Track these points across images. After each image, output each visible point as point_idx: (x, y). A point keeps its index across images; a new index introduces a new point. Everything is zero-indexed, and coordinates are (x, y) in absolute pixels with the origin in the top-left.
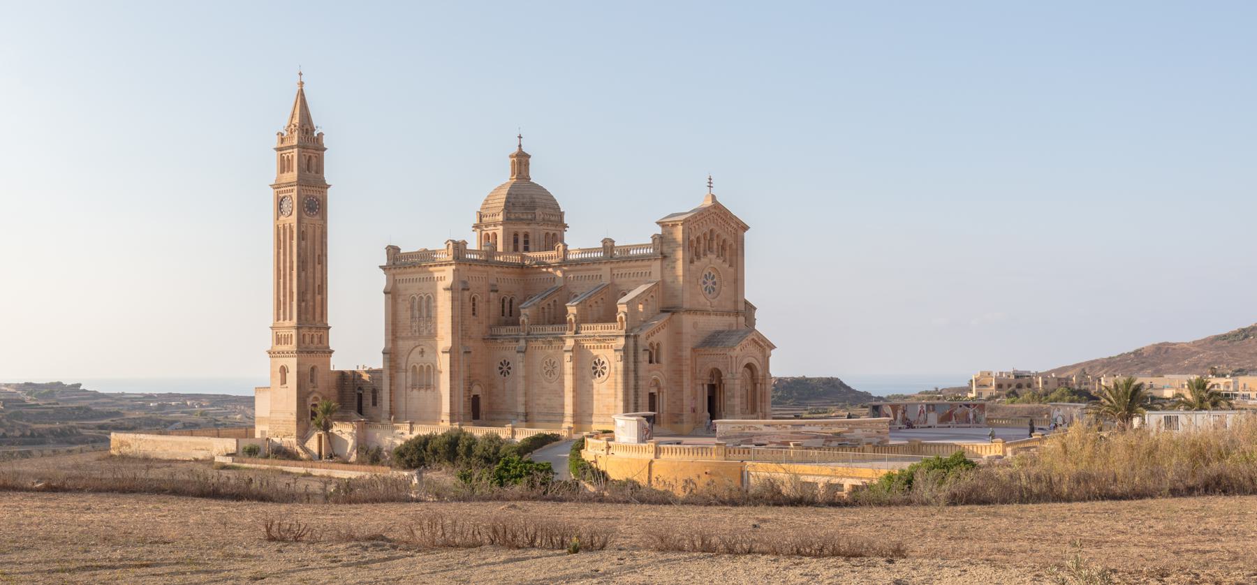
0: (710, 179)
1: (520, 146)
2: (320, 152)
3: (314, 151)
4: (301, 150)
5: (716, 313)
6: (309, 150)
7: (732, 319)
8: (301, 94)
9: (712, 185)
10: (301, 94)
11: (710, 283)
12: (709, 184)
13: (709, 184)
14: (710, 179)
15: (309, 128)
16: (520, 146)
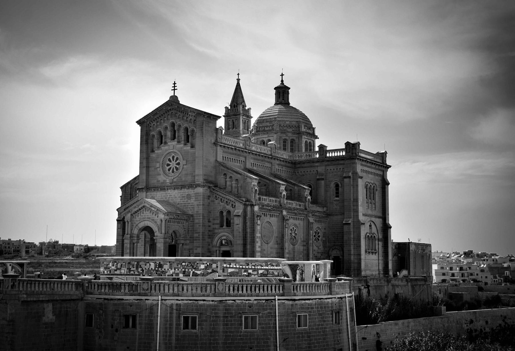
0: (175, 84)
1: (282, 81)
2: (238, 116)
3: (234, 117)
4: (227, 118)
5: (176, 187)
6: (231, 117)
7: (191, 191)
8: (238, 85)
9: (176, 88)
10: (238, 85)
11: (173, 164)
12: (173, 88)
13: (173, 88)
14: (175, 84)
15: (236, 104)
16: (282, 81)
